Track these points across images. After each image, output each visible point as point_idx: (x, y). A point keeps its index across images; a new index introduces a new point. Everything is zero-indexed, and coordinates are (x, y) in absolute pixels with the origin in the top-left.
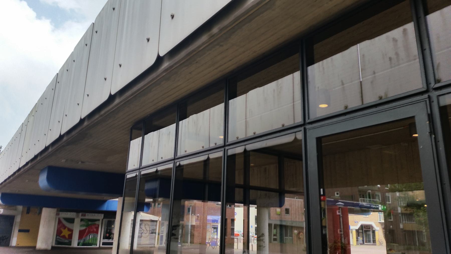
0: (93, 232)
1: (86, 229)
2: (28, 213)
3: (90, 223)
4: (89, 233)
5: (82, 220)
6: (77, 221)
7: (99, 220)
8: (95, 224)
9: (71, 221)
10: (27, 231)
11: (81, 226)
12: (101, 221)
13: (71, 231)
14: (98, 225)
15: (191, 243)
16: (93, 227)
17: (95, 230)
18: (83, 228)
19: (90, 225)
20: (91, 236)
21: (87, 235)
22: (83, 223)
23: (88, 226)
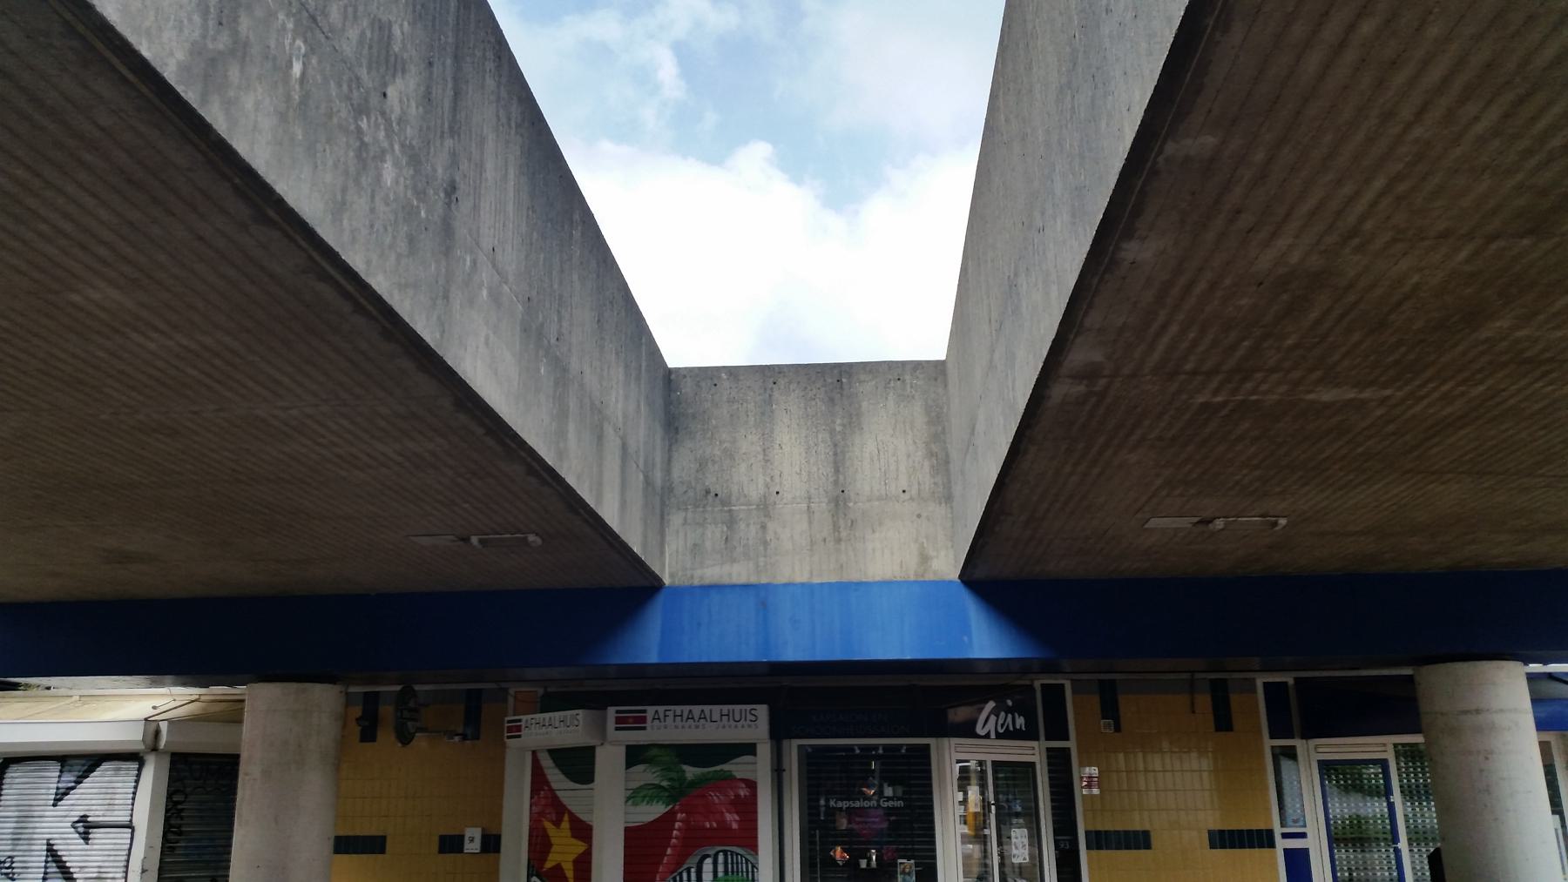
0: (723, 836)
1: (668, 818)
2: (368, 735)
3: (691, 772)
4: (696, 841)
5: (635, 755)
6: (609, 760)
7: (750, 749)
8: (729, 778)
9: (578, 764)
10: (373, 845)
11: (635, 796)
12: (765, 751)
13: (583, 831)
14: (752, 785)
15: (1303, 835)
16: (715, 797)
17: (732, 819)
18: (652, 811)
19: (693, 784)
20: (708, 865)
21: (679, 861)
22: (645, 775)
23: (677, 793)
